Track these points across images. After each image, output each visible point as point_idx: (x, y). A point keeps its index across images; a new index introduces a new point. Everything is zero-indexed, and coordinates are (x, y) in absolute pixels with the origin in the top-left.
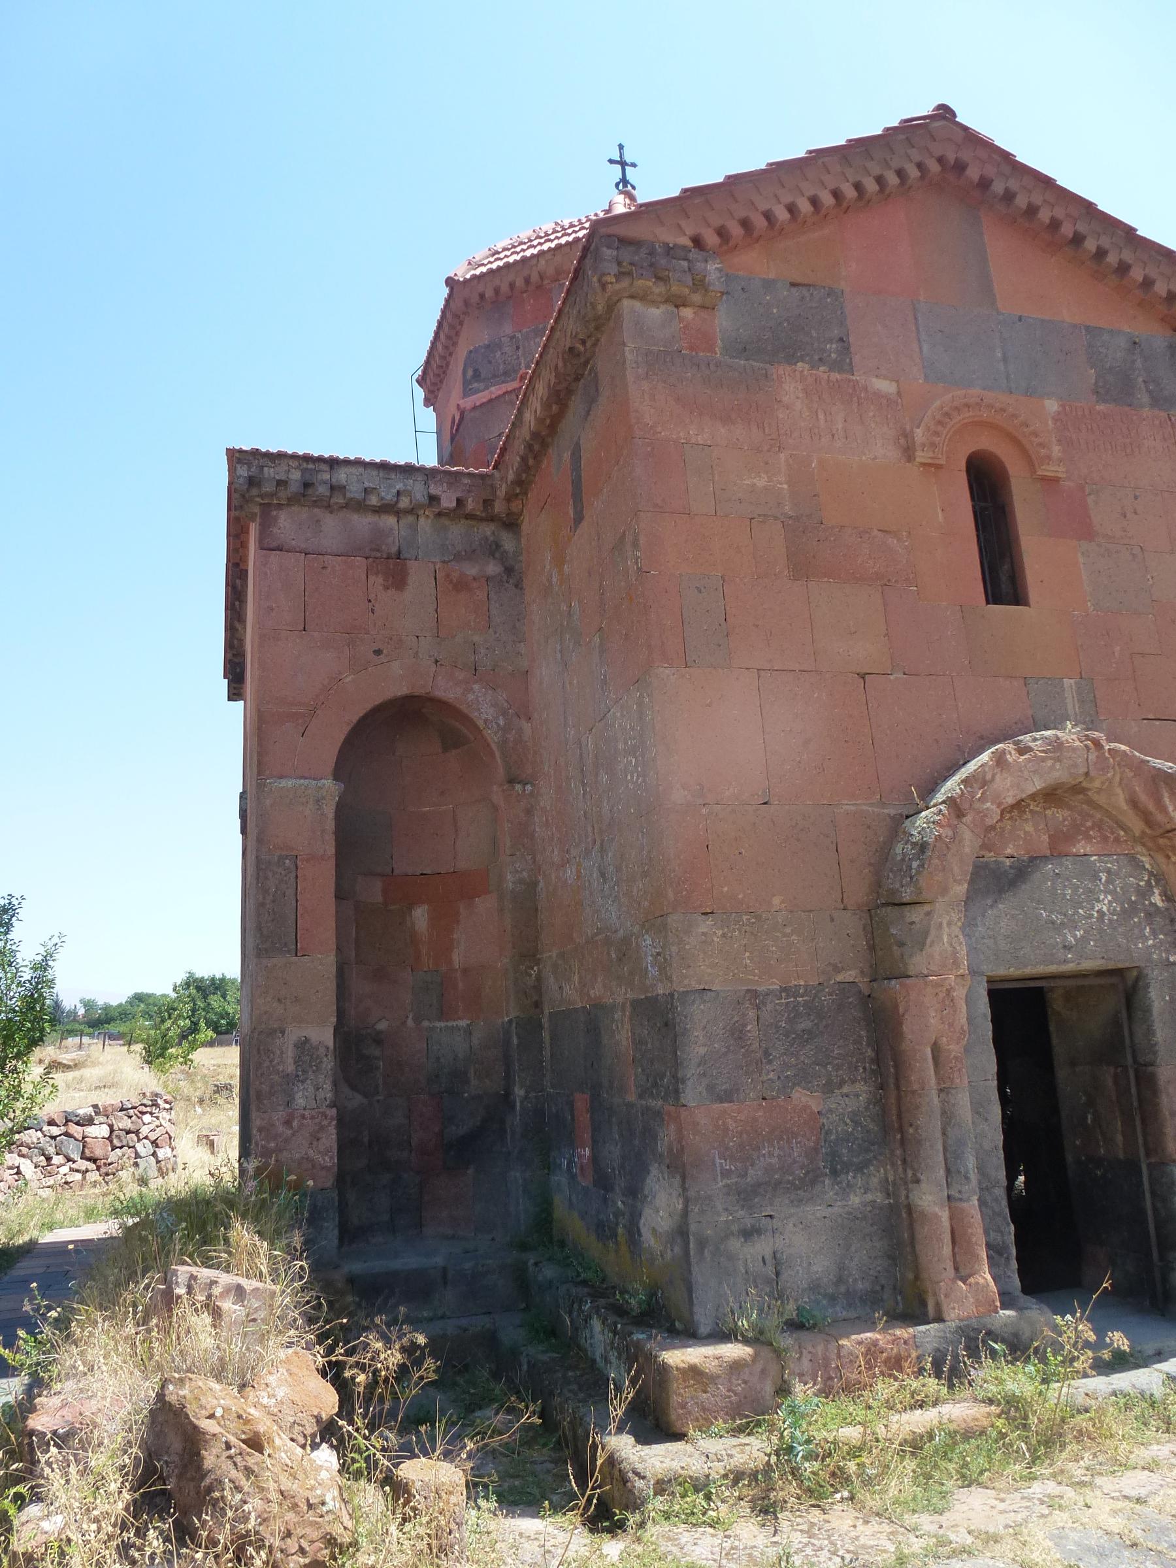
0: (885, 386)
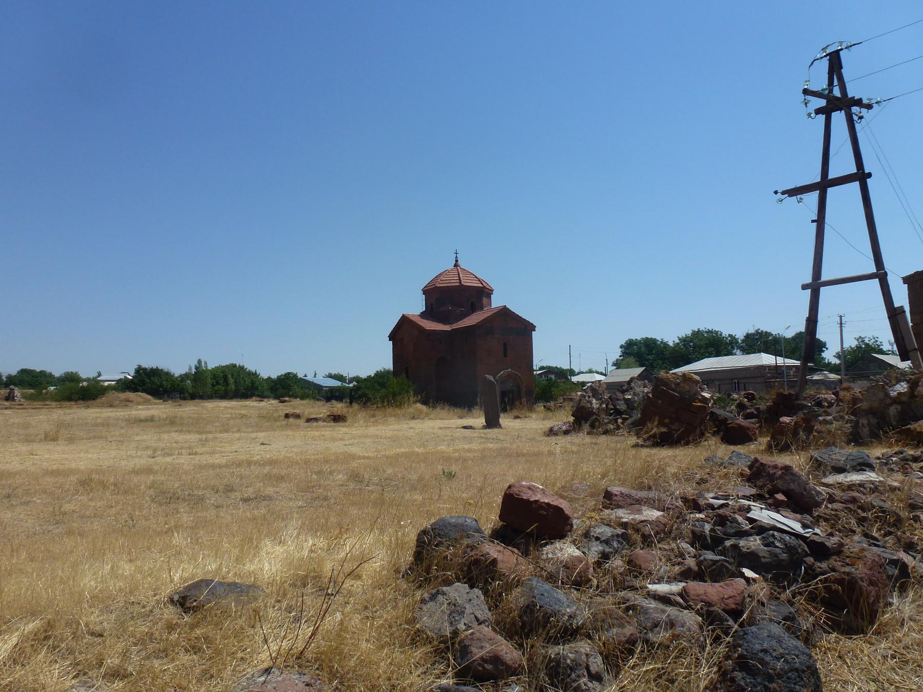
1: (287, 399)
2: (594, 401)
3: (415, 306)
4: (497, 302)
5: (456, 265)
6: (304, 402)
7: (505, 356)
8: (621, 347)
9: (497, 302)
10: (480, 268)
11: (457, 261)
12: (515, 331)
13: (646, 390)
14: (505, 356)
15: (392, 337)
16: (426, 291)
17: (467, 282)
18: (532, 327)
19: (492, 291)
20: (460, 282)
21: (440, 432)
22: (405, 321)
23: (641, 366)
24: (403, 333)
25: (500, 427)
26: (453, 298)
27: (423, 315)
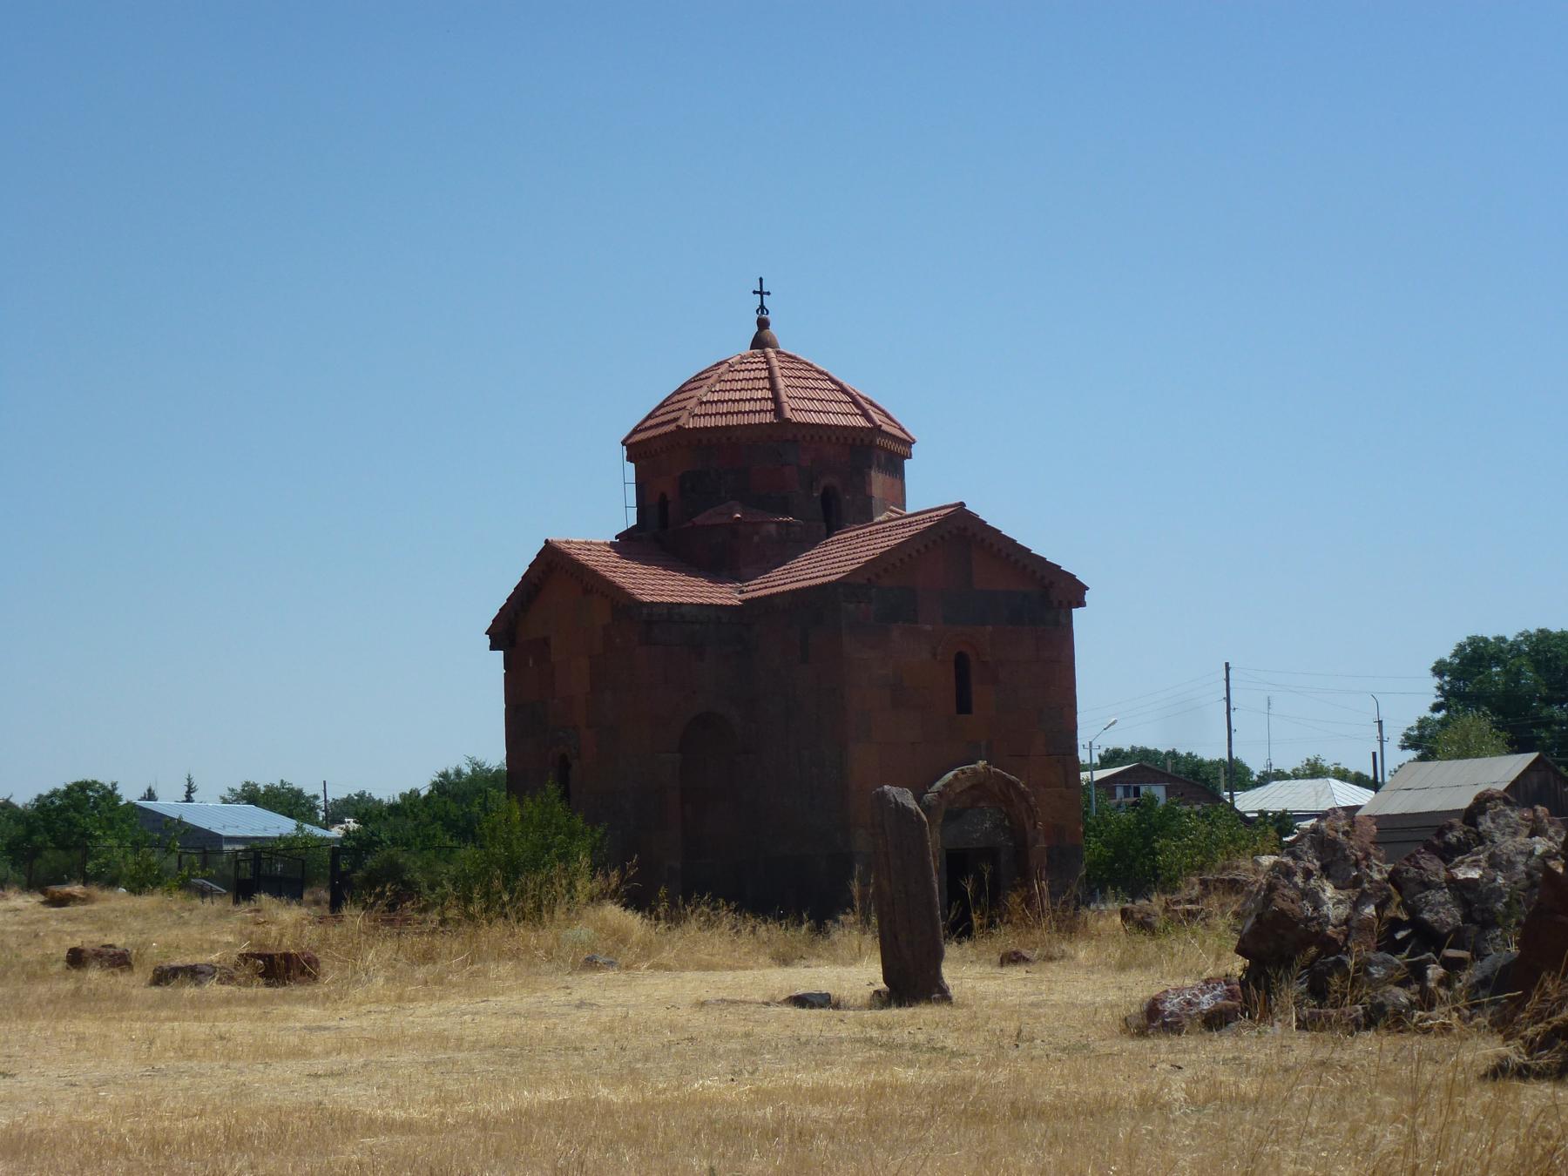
0: (928, 627)
1: (76, 889)
2: (1329, 891)
3: (597, 507)
4: (927, 487)
5: (760, 342)
6: (145, 902)
7: (964, 705)
8: (1439, 669)
9: (927, 487)
10: (858, 350)
11: (763, 324)
12: (1001, 611)
13: (1541, 845)
15: (503, 633)
16: (639, 449)
17: (804, 409)
18: (1070, 592)
19: (908, 443)
20: (778, 410)
21: (699, 1019)
22: (553, 567)
23: (1518, 745)
24: (547, 617)
25: (945, 997)
26: (745, 473)
27: (627, 544)
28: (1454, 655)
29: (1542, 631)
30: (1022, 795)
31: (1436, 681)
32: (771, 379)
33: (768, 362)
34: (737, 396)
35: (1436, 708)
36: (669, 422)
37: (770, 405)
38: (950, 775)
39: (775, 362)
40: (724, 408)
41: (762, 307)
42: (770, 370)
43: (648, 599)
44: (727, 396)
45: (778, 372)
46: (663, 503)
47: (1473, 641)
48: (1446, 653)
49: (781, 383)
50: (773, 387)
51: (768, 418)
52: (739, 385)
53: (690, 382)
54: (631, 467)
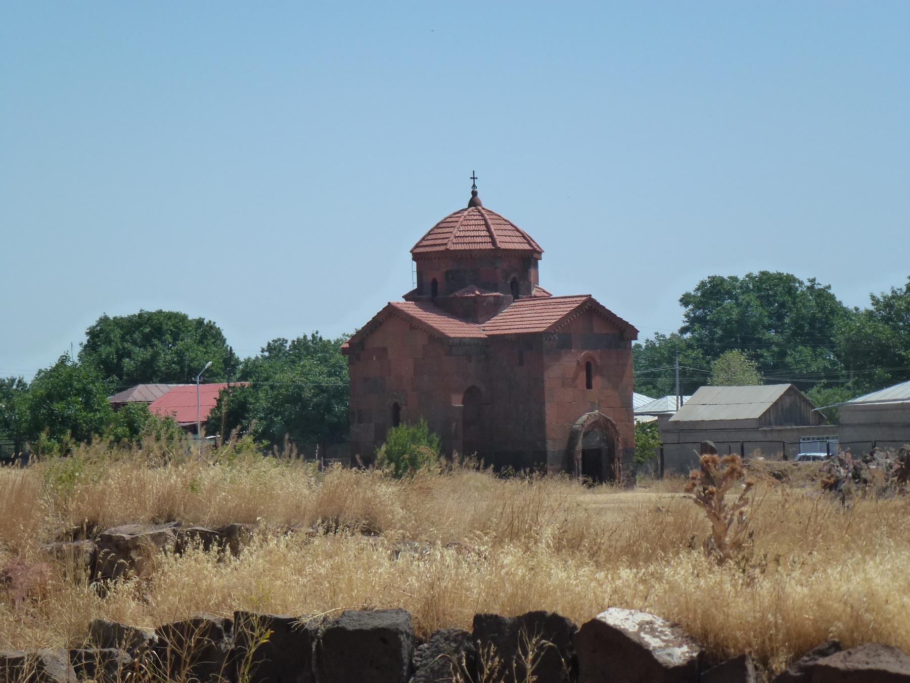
2: (842, 470)
3: (399, 281)
5: (474, 203)
7: (589, 386)
8: (686, 300)
9: (560, 279)
11: (474, 194)
13: (889, 461)
14: (589, 386)
20: (494, 242)
28: (697, 290)
29: (764, 273)
30: (612, 425)
31: (684, 310)
32: (487, 225)
33: (482, 215)
34: (472, 234)
35: (684, 330)
36: (443, 244)
37: (489, 239)
38: (585, 417)
39: (487, 217)
40: (467, 240)
41: (474, 185)
42: (485, 220)
43: (452, 336)
44: (468, 234)
45: (490, 222)
46: (434, 283)
47: (713, 279)
48: (691, 286)
49: (492, 228)
50: (489, 230)
51: (490, 246)
52: (472, 228)
53: (442, 222)
54: (415, 263)
